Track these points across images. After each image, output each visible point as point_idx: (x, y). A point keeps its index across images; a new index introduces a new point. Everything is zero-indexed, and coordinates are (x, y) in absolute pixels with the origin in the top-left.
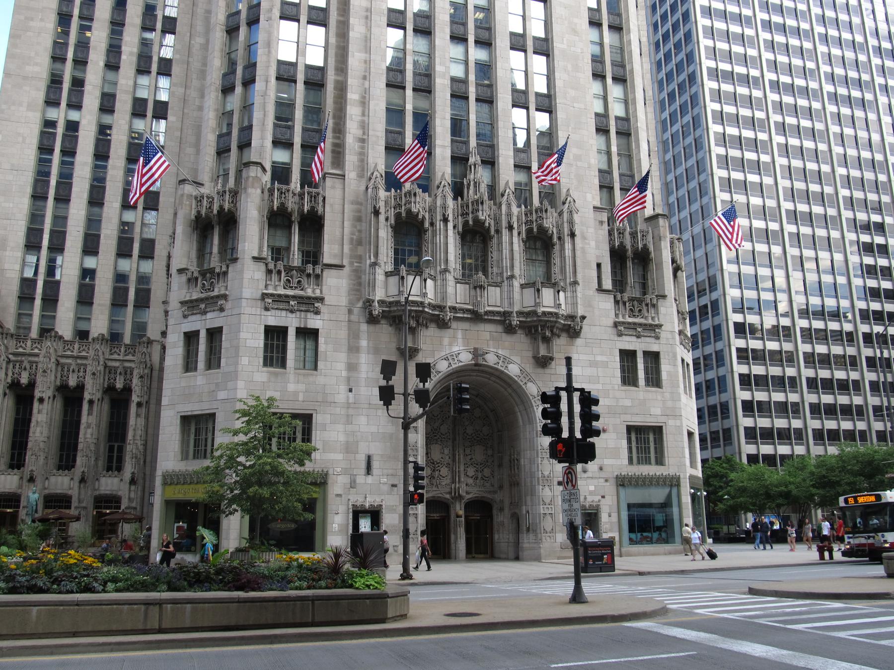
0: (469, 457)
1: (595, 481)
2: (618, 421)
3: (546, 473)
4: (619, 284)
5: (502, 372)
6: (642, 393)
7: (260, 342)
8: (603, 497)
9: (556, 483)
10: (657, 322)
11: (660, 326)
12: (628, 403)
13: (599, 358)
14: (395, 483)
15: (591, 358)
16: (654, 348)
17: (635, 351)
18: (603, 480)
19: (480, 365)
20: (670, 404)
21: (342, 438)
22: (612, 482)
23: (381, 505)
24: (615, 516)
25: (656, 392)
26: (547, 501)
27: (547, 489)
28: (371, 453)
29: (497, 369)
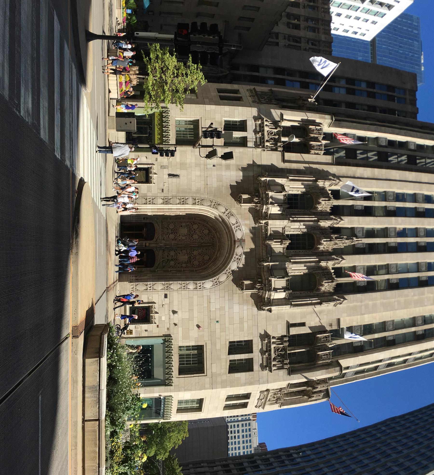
0: (181, 252)
1: (167, 321)
2: (206, 338)
3: (172, 287)
4: (295, 341)
5: (232, 258)
6: (225, 357)
7: (237, 119)
8: (158, 326)
9: (166, 293)
10: (274, 368)
11: (271, 371)
12: (218, 346)
13: (246, 325)
14: (164, 191)
15: (245, 319)
16: (256, 367)
17: (252, 352)
18: (168, 326)
19: (235, 244)
20: (219, 379)
21: (188, 161)
22: (166, 332)
23: (151, 183)
24: (146, 334)
25: (226, 368)
26: (155, 287)
27: (162, 287)
28: (181, 177)
29: (233, 255)
